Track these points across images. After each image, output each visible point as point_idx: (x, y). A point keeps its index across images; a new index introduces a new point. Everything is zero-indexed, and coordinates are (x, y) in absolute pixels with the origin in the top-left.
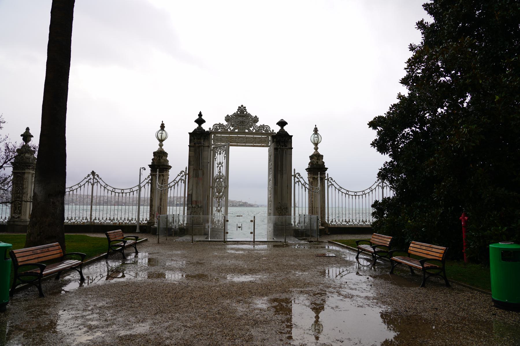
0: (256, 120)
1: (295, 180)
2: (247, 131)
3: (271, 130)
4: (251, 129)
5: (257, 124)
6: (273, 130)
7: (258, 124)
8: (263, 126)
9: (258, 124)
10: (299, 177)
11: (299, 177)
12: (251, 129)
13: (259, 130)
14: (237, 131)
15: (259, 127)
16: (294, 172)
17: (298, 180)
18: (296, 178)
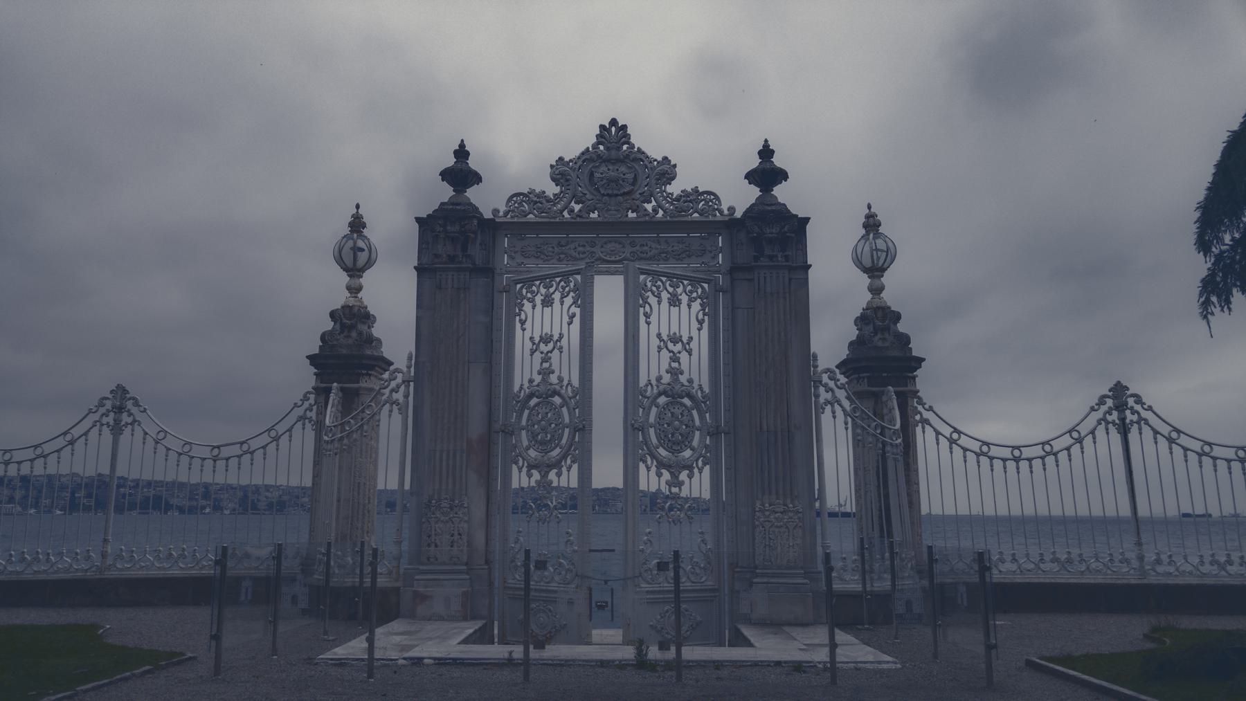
0: (666, 171)
1: (817, 396)
2: (631, 215)
3: (725, 207)
4: (649, 207)
5: (669, 189)
6: (732, 209)
7: (675, 188)
8: (693, 197)
9: (675, 188)
10: (831, 384)
11: (831, 384)
12: (649, 207)
13: (680, 210)
14: (594, 215)
15: (678, 199)
16: (816, 367)
17: (829, 396)
18: (822, 389)
